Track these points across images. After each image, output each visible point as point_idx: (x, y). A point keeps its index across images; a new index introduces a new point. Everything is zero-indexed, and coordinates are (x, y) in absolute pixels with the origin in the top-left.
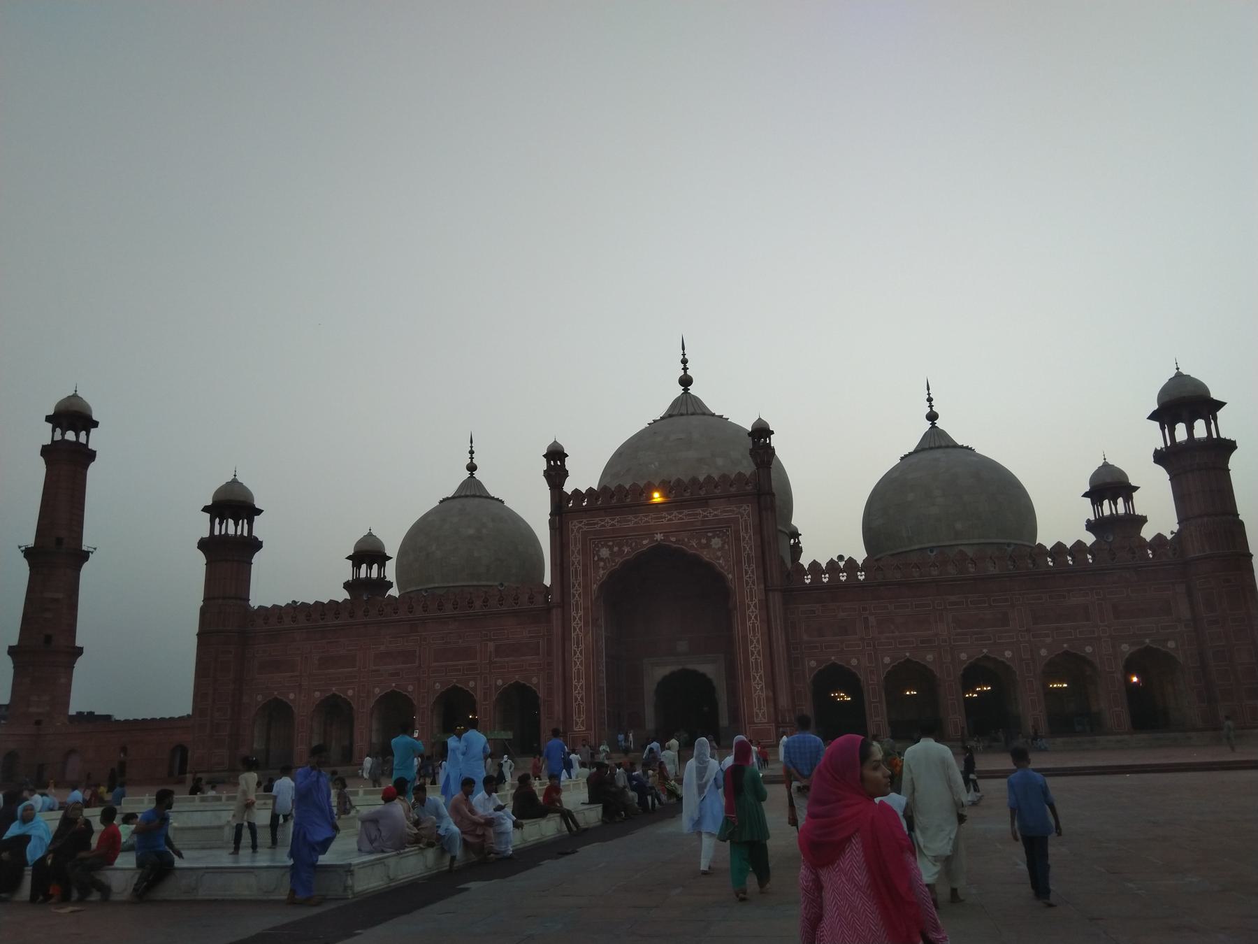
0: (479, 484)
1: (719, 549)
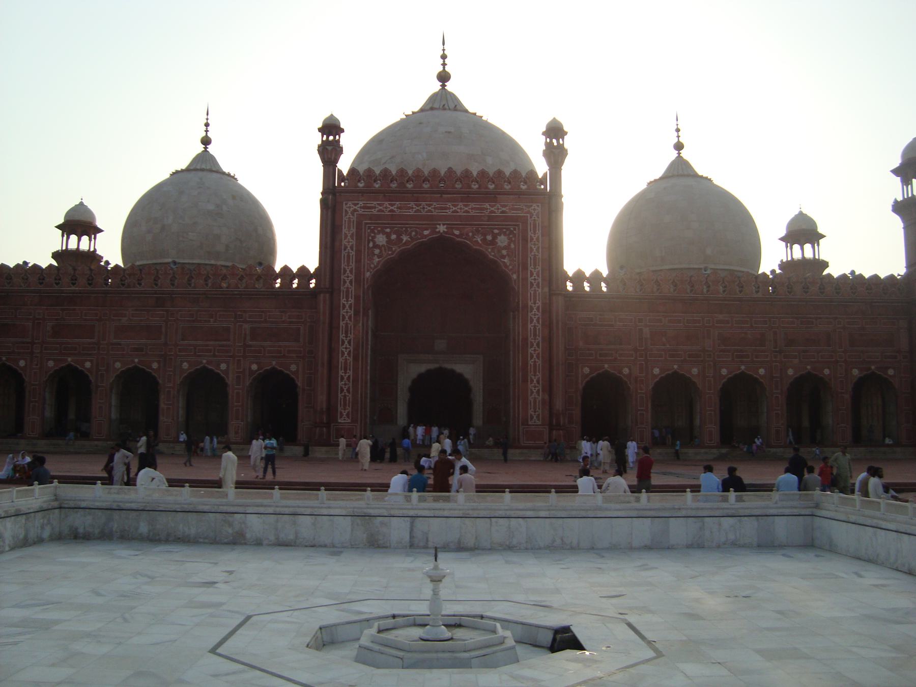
0: (212, 159)
1: (505, 248)
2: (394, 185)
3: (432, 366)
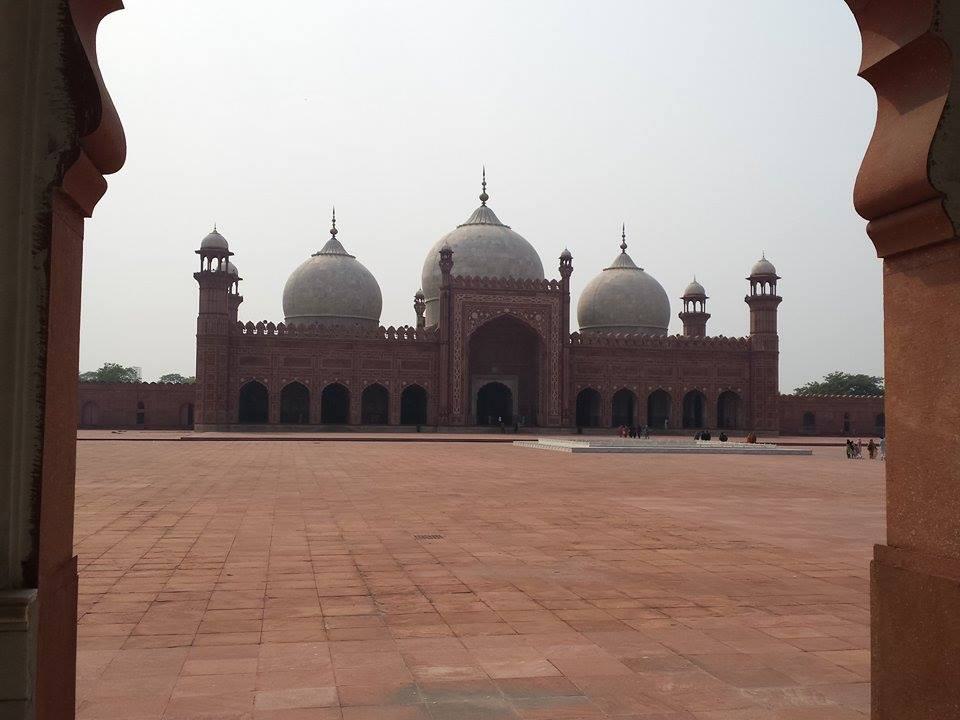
2: (482, 286)
3: (492, 381)
